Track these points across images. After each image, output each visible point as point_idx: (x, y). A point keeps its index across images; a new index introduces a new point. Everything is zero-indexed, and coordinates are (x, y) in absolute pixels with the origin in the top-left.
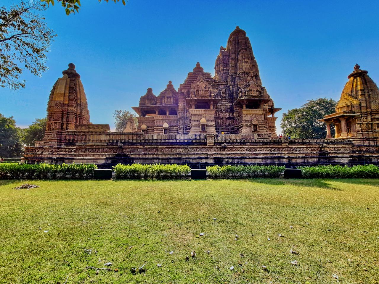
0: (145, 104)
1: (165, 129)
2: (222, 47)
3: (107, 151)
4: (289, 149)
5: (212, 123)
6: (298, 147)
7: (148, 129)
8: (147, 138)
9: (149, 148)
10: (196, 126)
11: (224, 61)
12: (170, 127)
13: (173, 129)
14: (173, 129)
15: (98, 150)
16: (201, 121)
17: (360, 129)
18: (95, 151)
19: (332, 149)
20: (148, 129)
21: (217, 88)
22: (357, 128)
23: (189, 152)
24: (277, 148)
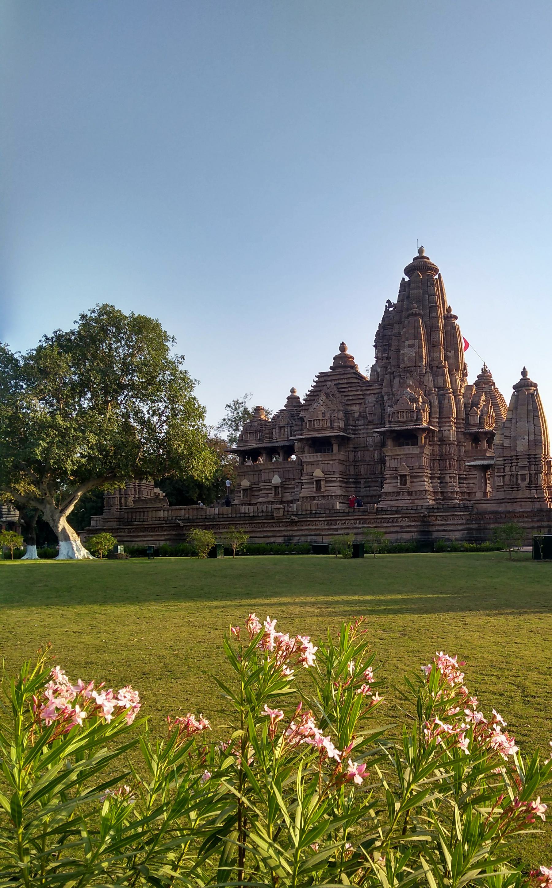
0: (246, 442)
1: (275, 487)
3: (166, 530)
4: (378, 521)
8: (208, 513)
9: (211, 525)
11: (388, 337)
12: (284, 483)
13: (290, 486)
14: (290, 486)
16: (314, 474)
21: (360, 404)
22: (497, 482)
24: (363, 519)
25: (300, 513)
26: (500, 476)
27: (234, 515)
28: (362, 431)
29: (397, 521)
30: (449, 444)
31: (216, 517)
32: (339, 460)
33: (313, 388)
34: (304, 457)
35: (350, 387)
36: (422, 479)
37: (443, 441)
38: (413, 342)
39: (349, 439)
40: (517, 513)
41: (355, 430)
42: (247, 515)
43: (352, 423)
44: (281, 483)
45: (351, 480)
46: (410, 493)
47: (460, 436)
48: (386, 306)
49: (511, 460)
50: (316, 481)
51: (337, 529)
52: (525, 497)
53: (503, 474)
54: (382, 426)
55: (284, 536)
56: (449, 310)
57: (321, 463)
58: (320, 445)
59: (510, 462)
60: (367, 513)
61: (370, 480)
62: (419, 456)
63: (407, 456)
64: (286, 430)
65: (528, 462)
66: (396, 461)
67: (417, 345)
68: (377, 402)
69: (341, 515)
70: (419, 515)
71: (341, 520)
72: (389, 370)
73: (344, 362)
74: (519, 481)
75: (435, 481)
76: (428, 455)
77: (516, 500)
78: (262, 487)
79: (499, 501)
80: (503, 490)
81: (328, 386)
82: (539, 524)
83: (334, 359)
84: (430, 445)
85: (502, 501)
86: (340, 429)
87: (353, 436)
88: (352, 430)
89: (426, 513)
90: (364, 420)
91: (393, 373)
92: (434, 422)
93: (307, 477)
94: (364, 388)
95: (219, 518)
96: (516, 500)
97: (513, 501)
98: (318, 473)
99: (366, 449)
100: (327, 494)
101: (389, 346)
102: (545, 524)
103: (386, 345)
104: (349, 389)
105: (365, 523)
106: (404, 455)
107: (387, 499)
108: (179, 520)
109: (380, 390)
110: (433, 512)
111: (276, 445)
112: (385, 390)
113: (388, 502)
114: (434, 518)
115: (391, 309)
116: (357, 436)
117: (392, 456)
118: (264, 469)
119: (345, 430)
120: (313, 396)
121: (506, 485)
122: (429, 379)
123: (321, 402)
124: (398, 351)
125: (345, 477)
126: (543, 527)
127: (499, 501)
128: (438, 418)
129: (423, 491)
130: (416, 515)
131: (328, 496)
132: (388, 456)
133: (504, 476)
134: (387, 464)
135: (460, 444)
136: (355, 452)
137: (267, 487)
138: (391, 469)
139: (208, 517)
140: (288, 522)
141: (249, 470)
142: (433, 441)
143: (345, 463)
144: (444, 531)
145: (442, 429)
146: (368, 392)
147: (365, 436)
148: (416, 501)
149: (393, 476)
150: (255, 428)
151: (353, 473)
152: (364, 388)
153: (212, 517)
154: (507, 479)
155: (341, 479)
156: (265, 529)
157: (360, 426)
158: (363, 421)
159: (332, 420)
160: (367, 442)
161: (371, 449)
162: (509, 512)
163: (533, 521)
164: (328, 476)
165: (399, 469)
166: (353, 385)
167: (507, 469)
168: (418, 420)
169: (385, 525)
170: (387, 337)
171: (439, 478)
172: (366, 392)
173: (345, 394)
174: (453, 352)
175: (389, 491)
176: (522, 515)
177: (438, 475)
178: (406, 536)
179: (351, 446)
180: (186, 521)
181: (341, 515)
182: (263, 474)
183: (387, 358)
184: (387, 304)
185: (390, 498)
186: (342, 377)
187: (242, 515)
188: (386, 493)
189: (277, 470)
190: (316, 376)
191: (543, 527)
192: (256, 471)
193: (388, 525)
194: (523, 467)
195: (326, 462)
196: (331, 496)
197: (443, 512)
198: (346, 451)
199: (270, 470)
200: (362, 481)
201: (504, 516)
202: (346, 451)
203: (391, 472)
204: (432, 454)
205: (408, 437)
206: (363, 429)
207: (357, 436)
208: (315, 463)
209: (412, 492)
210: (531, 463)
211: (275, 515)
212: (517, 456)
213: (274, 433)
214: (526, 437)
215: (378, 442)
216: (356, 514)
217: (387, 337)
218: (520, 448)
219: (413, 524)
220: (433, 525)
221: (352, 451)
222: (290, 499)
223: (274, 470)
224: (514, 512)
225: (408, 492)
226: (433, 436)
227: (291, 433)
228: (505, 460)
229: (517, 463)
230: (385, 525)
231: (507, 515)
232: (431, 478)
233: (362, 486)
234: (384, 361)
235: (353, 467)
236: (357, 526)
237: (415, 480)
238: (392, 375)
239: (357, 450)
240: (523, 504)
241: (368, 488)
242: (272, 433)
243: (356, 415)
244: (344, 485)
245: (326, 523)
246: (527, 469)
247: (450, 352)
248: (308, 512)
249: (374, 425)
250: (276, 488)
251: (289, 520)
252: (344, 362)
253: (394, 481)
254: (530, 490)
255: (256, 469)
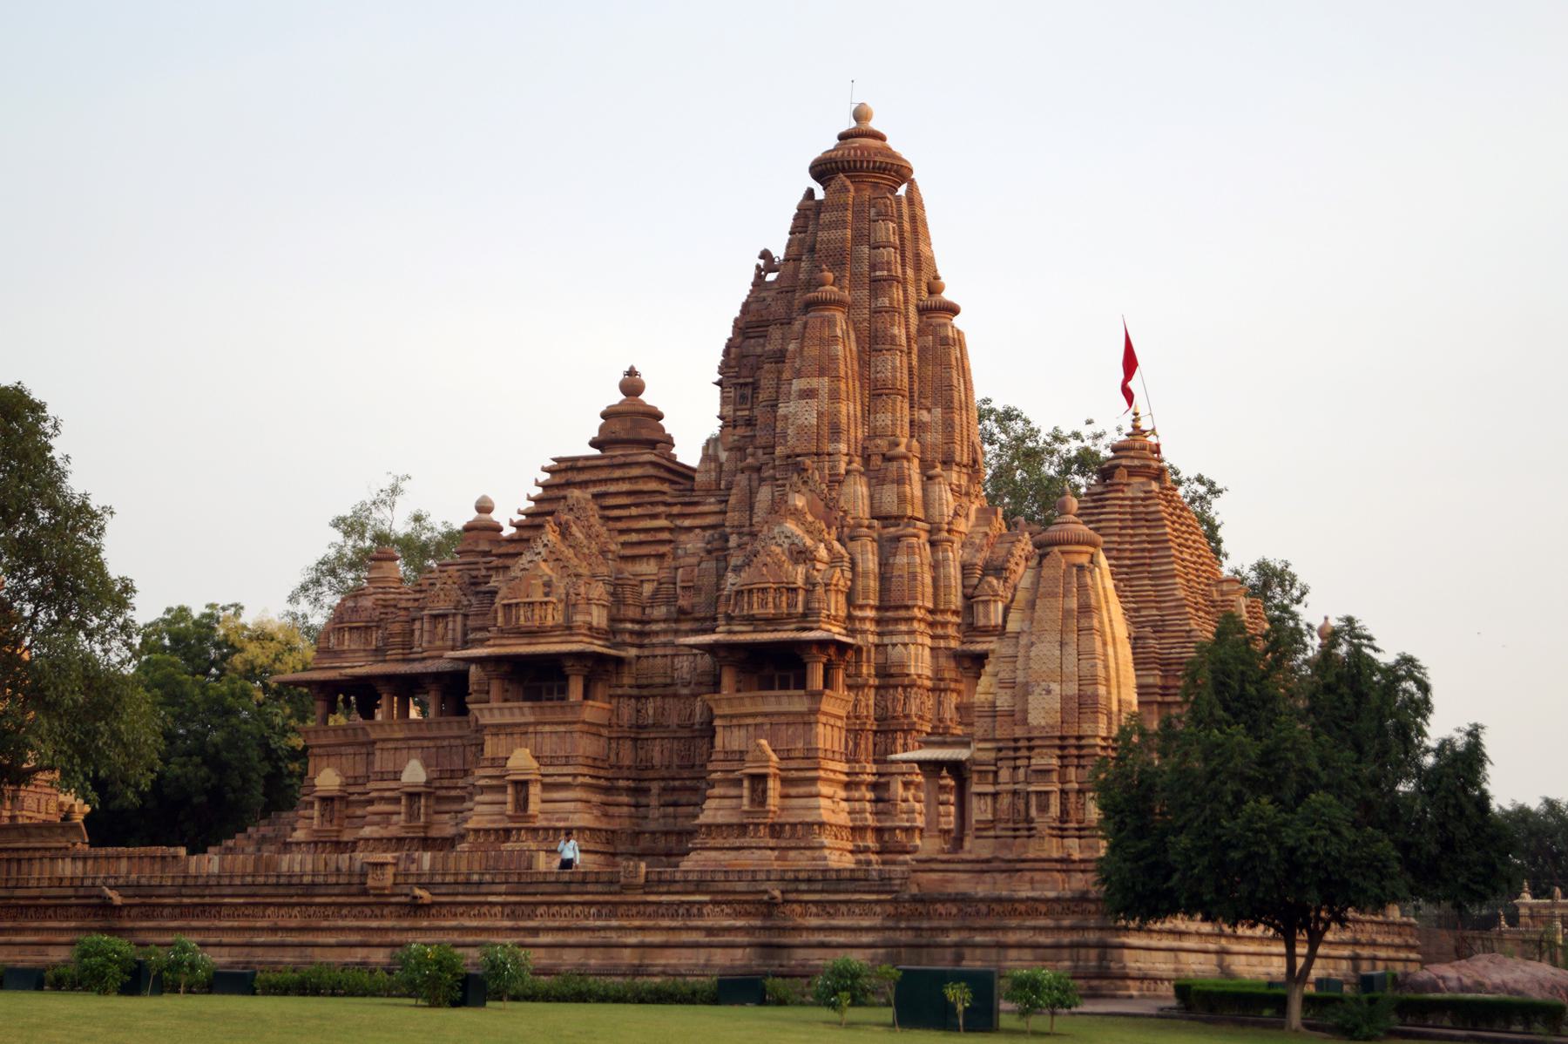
0: (337, 654)
1: (411, 795)
2: (765, 255)
4: (650, 909)
5: (565, 770)
6: (683, 903)
7: (351, 789)
10: (491, 788)
11: (754, 361)
13: (453, 793)
14: (453, 793)
15: (50, 912)
16: (510, 764)
17: (990, 817)
18: (44, 919)
19: (814, 909)
20: (351, 789)
21: (661, 556)
23: (314, 923)
25: (438, 879)
26: (985, 794)
27: (261, 880)
28: (662, 639)
29: (700, 915)
30: (905, 687)
31: (213, 881)
32: (584, 722)
33: (532, 504)
34: (486, 713)
35: (637, 505)
36: (813, 790)
37: (890, 678)
38: (815, 382)
39: (620, 661)
40: (1021, 901)
41: (641, 634)
42: (295, 880)
43: (632, 612)
44: (428, 783)
45: (621, 783)
46: (776, 830)
47: (943, 661)
48: (758, 267)
49: (1016, 749)
50: (516, 783)
51: (535, 931)
52: (1044, 855)
53: (990, 789)
54: (708, 624)
55: (393, 945)
56: (934, 288)
57: (531, 729)
58: (537, 678)
59: (1011, 754)
60: (616, 888)
61: (677, 783)
62: (807, 721)
63: (775, 719)
64: (450, 626)
65: (1060, 757)
66: (743, 732)
67: (824, 393)
68: (709, 552)
69: (549, 889)
70: (759, 897)
71: (548, 904)
72: (750, 460)
73: (632, 426)
74: (1033, 812)
75: (857, 795)
76: (840, 718)
77: (1019, 866)
78: (374, 794)
79: (978, 867)
80: (992, 833)
81: (570, 502)
82: (1075, 937)
83: (604, 415)
84: (850, 687)
85: (984, 866)
86: (593, 631)
87: (633, 652)
88: (632, 633)
89: (777, 893)
90: (667, 603)
91: (759, 470)
92: (863, 619)
93: (490, 772)
94: (676, 510)
95: (219, 885)
96: (1019, 866)
97: (1012, 868)
98: (521, 760)
99: (670, 690)
100: (545, 824)
101: (755, 386)
102: (1092, 937)
103: (746, 384)
104: (634, 511)
105: (610, 916)
106: (766, 715)
107: (711, 843)
108: (111, 888)
109: (721, 517)
110: (797, 891)
111: (417, 668)
112: (733, 517)
113: (713, 854)
114: (798, 908)
115: (771, 277)
116: (646, 652)
117: (733, 716)
118: (384, 740)
119: (609, 634)
120: (532, 523)
121: (1000, 820)
122: (857, 494)
123: (544, 551)
124: (775, 406)
125: (602, 773)
126: (1086, 946)
127: (978, 867)
128: (878, 609)
129: (813, 824)
130: (749, 897)
131: (546, 829)
132: (723, 717)
133: (995, 795)
134: (718, 741)
135: (942, 685)
136: (638, 698)
137: (387, 794)
138: (729, 755)
139: (190, 882)
140: (405, 904)
141: (342, 739)
142: (859, 675)
143: (605, 732)
144: (823, 945)
145: (886, 640)
146: (687, 523)
147: (669, 651)
148: (792, 854)
149: (731, 776)
150: (364, 615)
151: (627, 763)
152: (676, 510)
153: (200, 881)
154: (1005, 801)
155: (588, 780)
156: (341, 923)
157: (657, 621)
158: (664, 609)
159: (570, 606)
160: (673, 669)
161: (685, 691)
162: (999, 900)
163: (1059, 928)
164: (551, 770)
165: (747, 758)
166: (646, 499)
167: (1004, 775)
168: (807, 617)
169: (666, 923)
170: (752, 360)
171: (874, 787)
172: (678, 522)
173: (621, 525)
174: (938, 411)
175: (720, 820)
176: (1033, 907)
177: (870, 778)
178: (720, 958)
179: (627, 680)
180: (130, 892)
181: (549, 889)
182: (378, 753)
183: (750, 422)
184: (761, 262)
185: (719, 842)
186: (618, 473)
187: (282, 880)
188: (709, 826)
189: (417, 743)
190: (544, 470)
191: (1086, 946)
192: (363, 744)
193: (674, 924)
194: (1044, 773)
195: (547, 728)
196: (557, 830)
197: (822, 891)
198: (611, 696)
199: (399, 744)
200: (655, 787)
201: (983, 908)
202: (611, 696)
203: (728, 766)
204: (854, 716)
205: (778, 665)
206: (665, 632)
207: (646, 652)
208: (516, 730)
209: (782, 825)
210: (1066, 762)
211: (370, 882)
212: (1030, 739)
213: (417, 633)
214: (1055, 687)
215: (703, 673)
216: (590, 888)
217: (752, 360)
218: (1035, 718)
219: (739, 923)
220: (794, 929)
221: (630, 697)
222: (449, 831)
223: (412, 743)
224: (1011, 900)
225: (772, 826)
226: (858, 663)
227: (465, 634)
228: (1000, 750)
229: (1029, 758)
230: (666, 923)
231: (993, 906)
232: (847, 786)
233: (654, 801)
234: (741, 431)
235: (628, 744)
236: (591, 923)
237: (793, 791)
238: (755, 476)
239: (645, 692)
240: (1038, 876)
241: (671, 809)
242: (413, 631)
243: (647, 589)
244: (596, 798)
245: (507, 910)
246: (1055, 777)
247: (929, 410)
248: (461, 878)
249: (696, 620)
250: (413, 796)
251: (407, 900)
252: (632, 426)
253: (733, 792)
254: (1062, 837)
255: (361, 738)
